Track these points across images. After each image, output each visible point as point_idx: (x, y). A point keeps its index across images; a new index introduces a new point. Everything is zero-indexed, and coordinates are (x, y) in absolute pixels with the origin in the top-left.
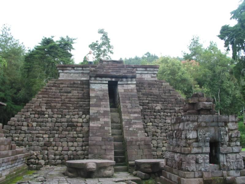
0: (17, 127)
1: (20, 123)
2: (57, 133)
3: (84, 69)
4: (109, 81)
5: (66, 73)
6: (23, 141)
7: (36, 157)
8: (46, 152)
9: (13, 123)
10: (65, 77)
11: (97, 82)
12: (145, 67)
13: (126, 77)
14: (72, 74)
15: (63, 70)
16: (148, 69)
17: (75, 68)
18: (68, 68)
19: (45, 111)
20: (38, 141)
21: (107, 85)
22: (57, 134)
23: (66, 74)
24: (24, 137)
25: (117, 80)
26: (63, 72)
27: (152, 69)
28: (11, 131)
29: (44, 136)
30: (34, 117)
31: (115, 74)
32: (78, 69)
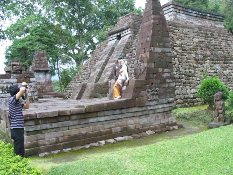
25: (120, 34)
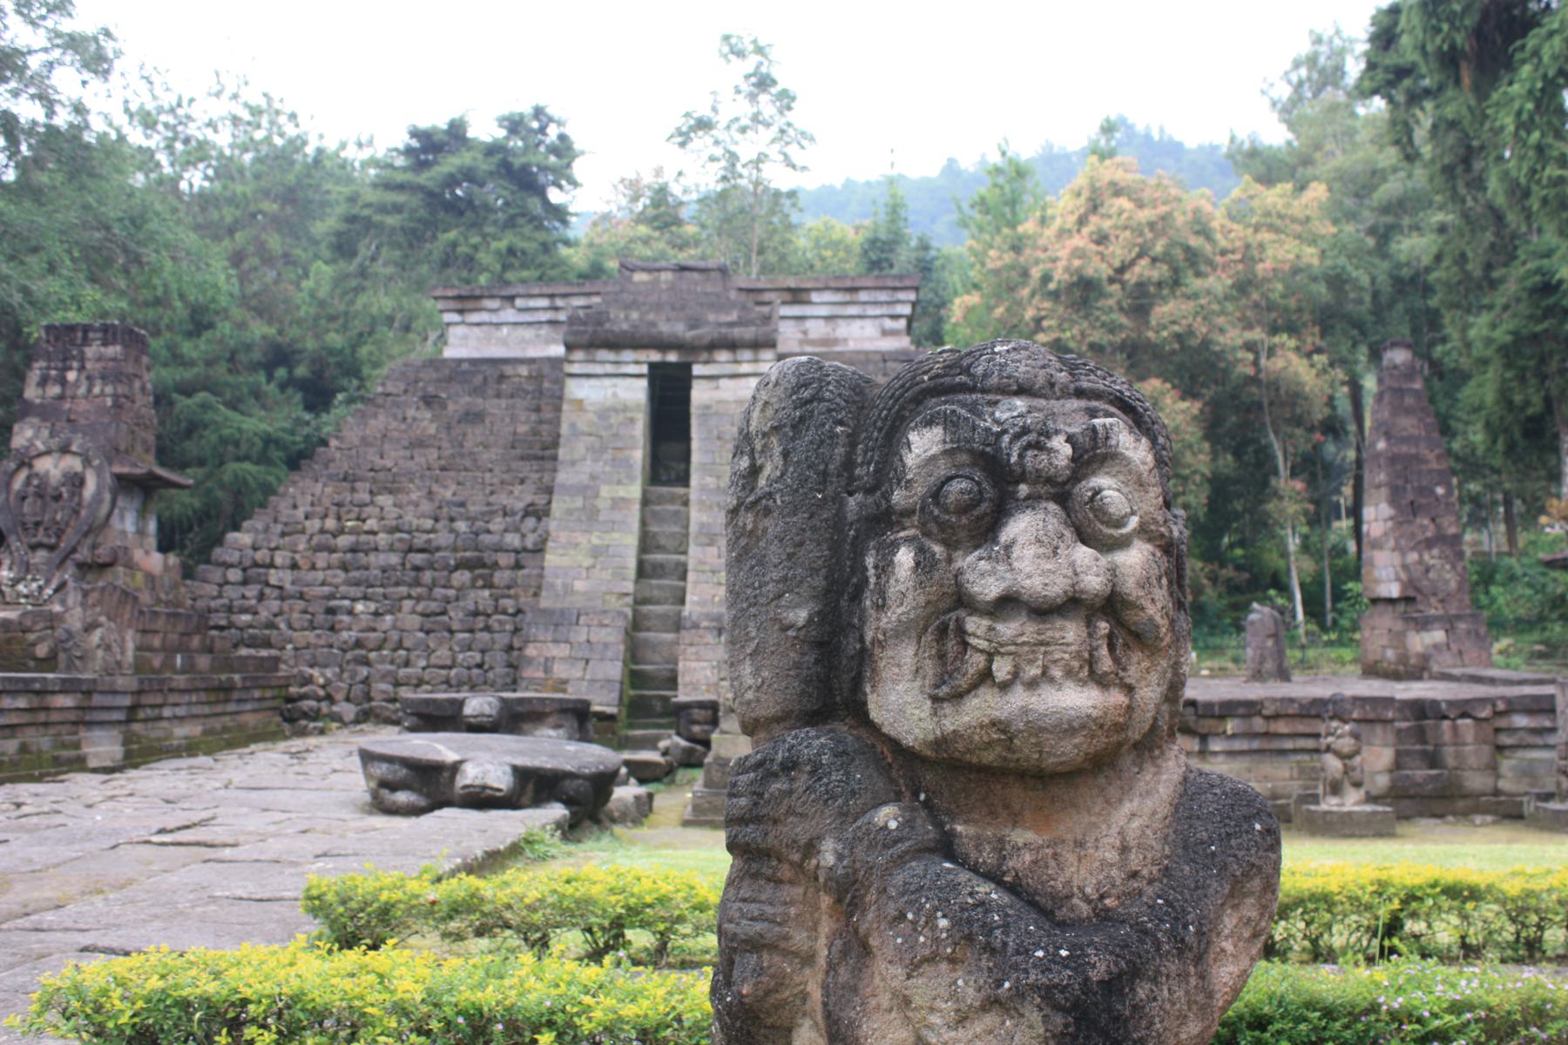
0: (253, 572)
1: (261, 556)
2: (414, 593)
3: (559, 302)
4: (652, 366)
5: (478, 324)
6: (271, 625)
7: (321, 693)
8: (364, 671)
9: (234, 557)
10: (472, 342)
11: (598, 369)
12: (848, 284)
13: (733, 346)
14: (505, 330)
15: (461, 312)
16: (863, 296)
17: (519, 302)
18: (489, 303)
19: (366, 505)
20: (332, 629)
21: (644, 383)
22: (409, 597)
23: (476, 330)
24: (276, 610)
25: (690, 359)
26: (463, 323)
27: (883, 296)
28: (226, 588)
29: (359, 607)
30: (322, 531)
31: (679, 329)
32: (532, 303)
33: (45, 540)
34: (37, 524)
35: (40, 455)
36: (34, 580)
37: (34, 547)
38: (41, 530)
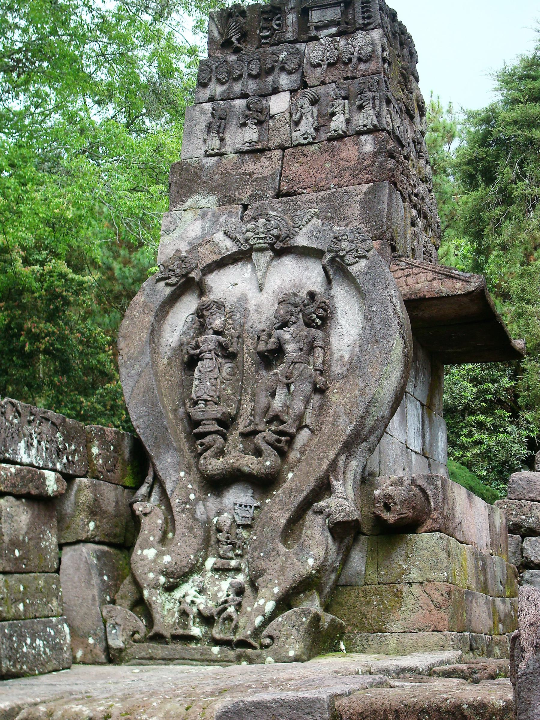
33: (249, 463)
34: (226, 423)
35: (221, 264)
36: (222, 571)
37: (216, 484)
38: (234, 436)
